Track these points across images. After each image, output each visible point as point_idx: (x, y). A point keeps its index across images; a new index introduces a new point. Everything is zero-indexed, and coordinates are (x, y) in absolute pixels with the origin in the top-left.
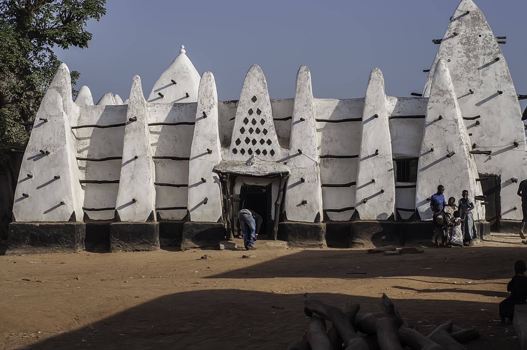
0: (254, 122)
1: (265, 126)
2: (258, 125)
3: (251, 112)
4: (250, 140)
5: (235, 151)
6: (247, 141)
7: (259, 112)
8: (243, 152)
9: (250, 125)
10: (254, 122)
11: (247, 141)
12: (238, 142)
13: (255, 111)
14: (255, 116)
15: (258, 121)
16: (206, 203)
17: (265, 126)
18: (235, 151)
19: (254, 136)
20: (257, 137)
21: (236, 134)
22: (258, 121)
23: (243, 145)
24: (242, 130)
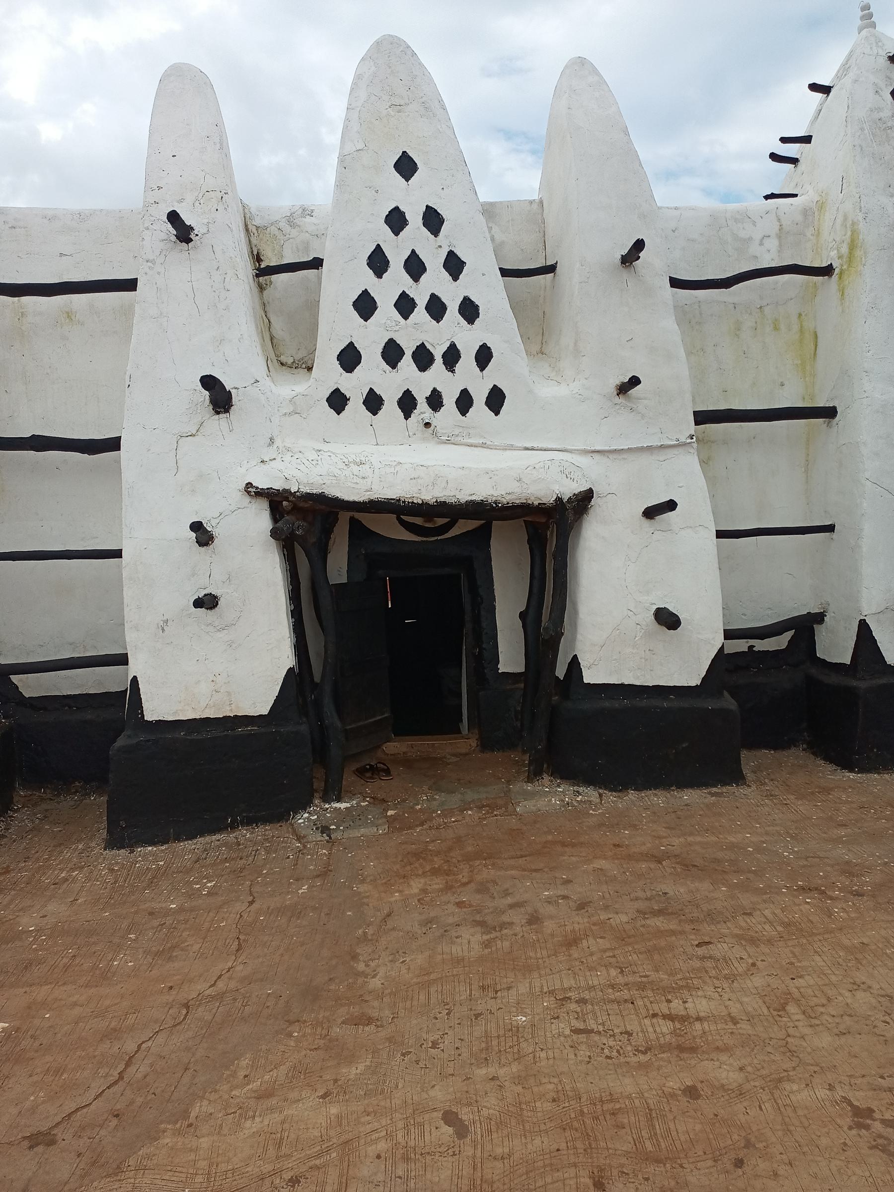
0: (415, 267)
1: (466, 286)
2: (433, 279)
3: (396, 220)
4: (400, 353)
5: (337, 401)
6: (392, 353)
7: (433, 220)
8: (373, 402)
9: (397, 280)
10: (415, 267)
11: (392, 353)
12: (350, 358)
13: (415, 218)
14: (416, 232)
15: (434, 262)
16: (219, 653)
17: (466, 286)
18: (337, 401)
19: (417, 330)
20: (438, 336)
21: (338, 325)
22: (434, 262)
23: (372, 373)
24: (365, 306)
